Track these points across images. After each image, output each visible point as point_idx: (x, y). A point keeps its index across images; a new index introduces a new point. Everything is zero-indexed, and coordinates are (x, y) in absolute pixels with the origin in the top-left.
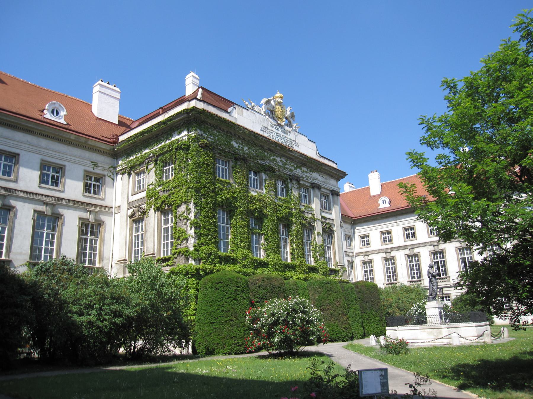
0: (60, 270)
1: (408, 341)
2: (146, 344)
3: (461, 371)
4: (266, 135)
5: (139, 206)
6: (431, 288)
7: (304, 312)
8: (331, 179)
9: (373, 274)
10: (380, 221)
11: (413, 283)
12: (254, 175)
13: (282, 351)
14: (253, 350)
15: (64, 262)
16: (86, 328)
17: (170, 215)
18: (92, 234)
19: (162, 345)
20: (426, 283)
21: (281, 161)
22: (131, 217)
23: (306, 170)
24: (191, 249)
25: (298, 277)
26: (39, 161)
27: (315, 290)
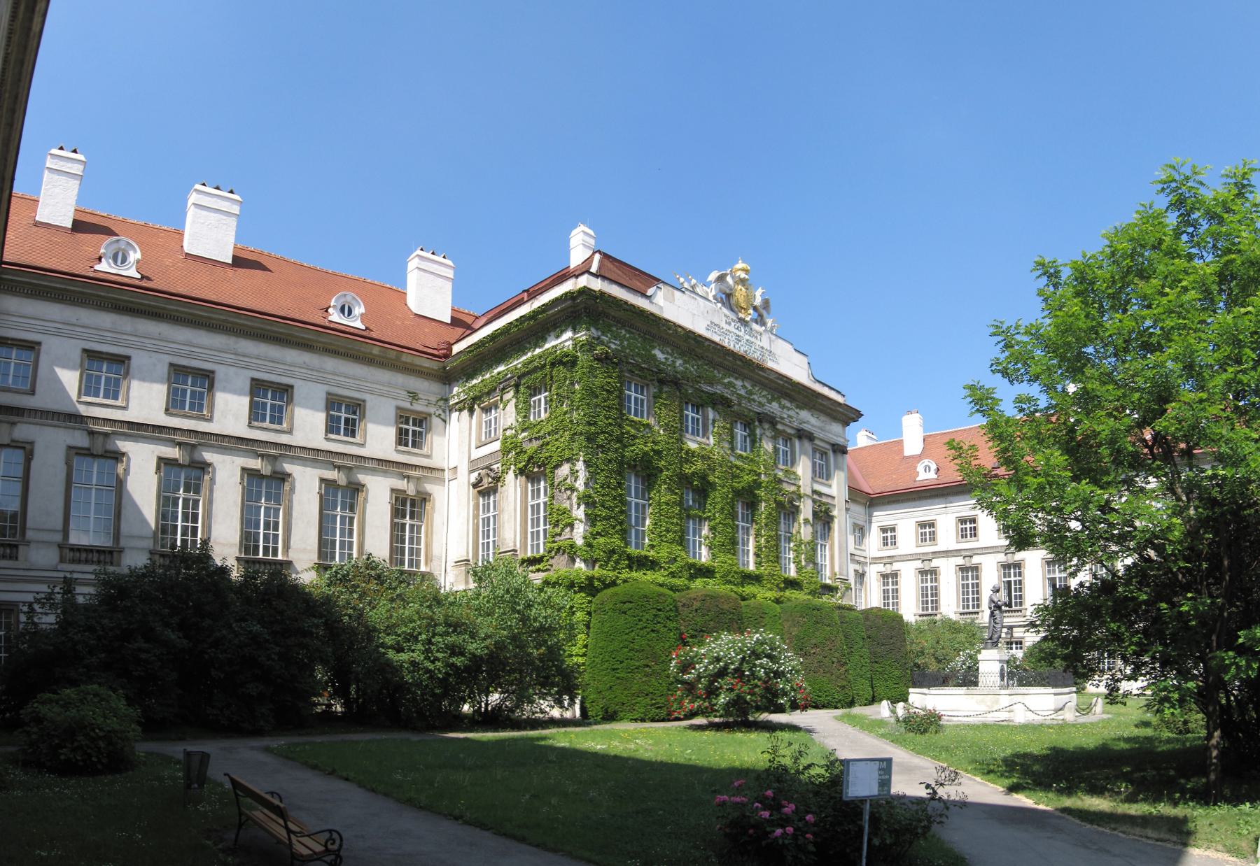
0: (364, 577)
1: (942, 713)
2: (504, 700)
3: (1017, 764)
4: (716, 338)
5: (488, 467)
6: (992, 628)
7: (769, 657)
8: (834, 424)
9: (897, 596)
10: (917, 503)
11: (965, 616)
12: (693, 412)
13: (731, 720)
14: (682, 717)
15: (370, 564)
16: (409, 672)
17: (542, 483)
18: (412, 517)
19: (531, 702)
20: (984, 617)
21: (744, 387)
22: (475, 486)
23: (788, 404)
24: (580, 542)
25: (766, 596)
27: (793, 620)
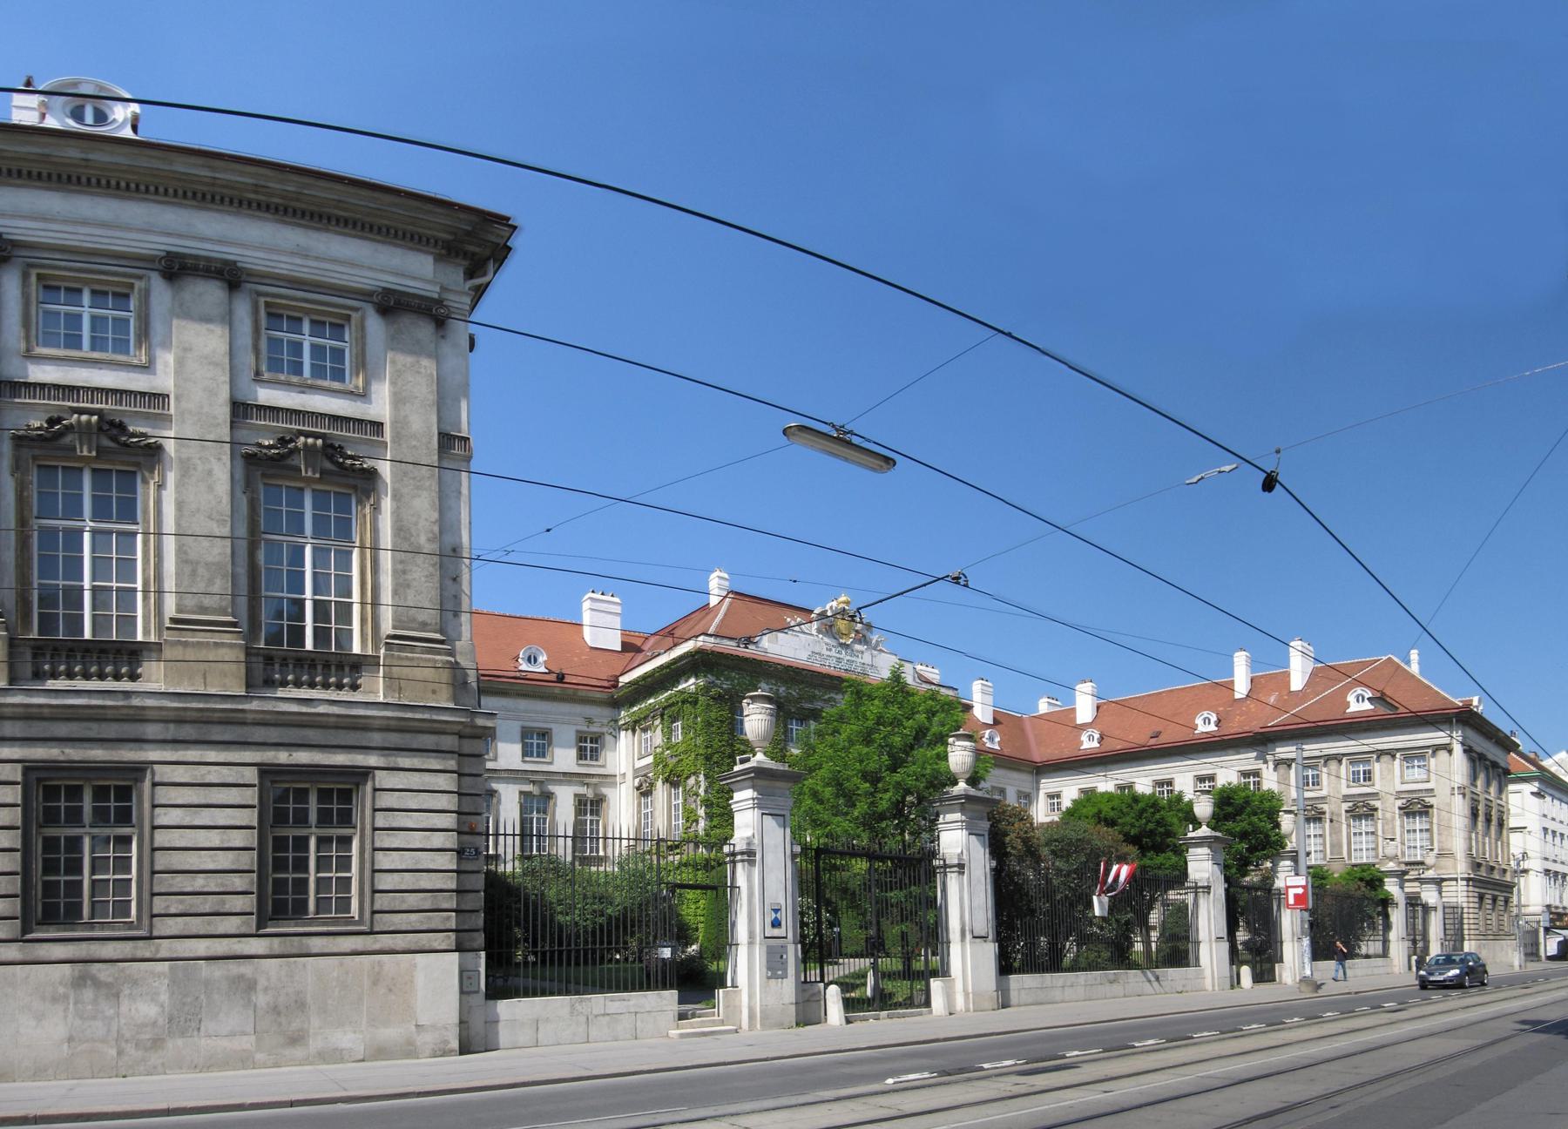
22: (638, 789)
26: (519, 729)
